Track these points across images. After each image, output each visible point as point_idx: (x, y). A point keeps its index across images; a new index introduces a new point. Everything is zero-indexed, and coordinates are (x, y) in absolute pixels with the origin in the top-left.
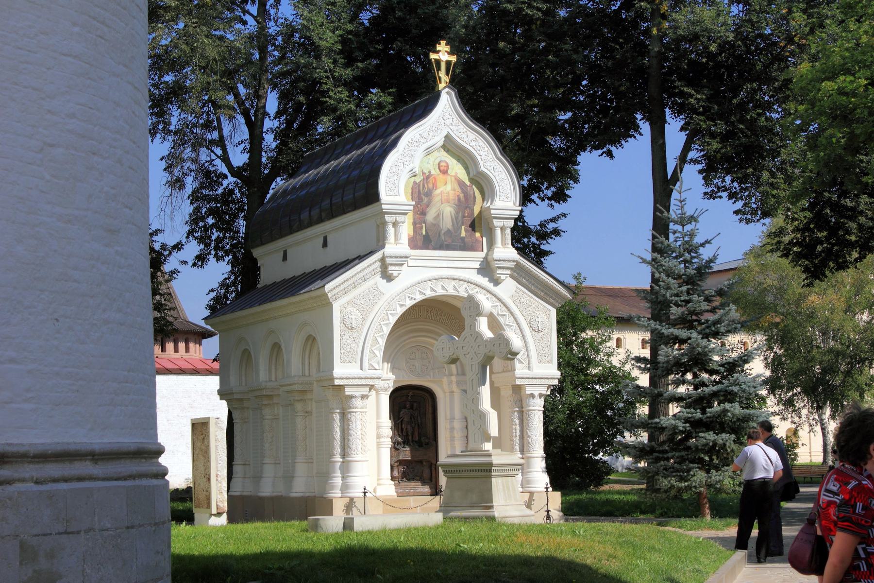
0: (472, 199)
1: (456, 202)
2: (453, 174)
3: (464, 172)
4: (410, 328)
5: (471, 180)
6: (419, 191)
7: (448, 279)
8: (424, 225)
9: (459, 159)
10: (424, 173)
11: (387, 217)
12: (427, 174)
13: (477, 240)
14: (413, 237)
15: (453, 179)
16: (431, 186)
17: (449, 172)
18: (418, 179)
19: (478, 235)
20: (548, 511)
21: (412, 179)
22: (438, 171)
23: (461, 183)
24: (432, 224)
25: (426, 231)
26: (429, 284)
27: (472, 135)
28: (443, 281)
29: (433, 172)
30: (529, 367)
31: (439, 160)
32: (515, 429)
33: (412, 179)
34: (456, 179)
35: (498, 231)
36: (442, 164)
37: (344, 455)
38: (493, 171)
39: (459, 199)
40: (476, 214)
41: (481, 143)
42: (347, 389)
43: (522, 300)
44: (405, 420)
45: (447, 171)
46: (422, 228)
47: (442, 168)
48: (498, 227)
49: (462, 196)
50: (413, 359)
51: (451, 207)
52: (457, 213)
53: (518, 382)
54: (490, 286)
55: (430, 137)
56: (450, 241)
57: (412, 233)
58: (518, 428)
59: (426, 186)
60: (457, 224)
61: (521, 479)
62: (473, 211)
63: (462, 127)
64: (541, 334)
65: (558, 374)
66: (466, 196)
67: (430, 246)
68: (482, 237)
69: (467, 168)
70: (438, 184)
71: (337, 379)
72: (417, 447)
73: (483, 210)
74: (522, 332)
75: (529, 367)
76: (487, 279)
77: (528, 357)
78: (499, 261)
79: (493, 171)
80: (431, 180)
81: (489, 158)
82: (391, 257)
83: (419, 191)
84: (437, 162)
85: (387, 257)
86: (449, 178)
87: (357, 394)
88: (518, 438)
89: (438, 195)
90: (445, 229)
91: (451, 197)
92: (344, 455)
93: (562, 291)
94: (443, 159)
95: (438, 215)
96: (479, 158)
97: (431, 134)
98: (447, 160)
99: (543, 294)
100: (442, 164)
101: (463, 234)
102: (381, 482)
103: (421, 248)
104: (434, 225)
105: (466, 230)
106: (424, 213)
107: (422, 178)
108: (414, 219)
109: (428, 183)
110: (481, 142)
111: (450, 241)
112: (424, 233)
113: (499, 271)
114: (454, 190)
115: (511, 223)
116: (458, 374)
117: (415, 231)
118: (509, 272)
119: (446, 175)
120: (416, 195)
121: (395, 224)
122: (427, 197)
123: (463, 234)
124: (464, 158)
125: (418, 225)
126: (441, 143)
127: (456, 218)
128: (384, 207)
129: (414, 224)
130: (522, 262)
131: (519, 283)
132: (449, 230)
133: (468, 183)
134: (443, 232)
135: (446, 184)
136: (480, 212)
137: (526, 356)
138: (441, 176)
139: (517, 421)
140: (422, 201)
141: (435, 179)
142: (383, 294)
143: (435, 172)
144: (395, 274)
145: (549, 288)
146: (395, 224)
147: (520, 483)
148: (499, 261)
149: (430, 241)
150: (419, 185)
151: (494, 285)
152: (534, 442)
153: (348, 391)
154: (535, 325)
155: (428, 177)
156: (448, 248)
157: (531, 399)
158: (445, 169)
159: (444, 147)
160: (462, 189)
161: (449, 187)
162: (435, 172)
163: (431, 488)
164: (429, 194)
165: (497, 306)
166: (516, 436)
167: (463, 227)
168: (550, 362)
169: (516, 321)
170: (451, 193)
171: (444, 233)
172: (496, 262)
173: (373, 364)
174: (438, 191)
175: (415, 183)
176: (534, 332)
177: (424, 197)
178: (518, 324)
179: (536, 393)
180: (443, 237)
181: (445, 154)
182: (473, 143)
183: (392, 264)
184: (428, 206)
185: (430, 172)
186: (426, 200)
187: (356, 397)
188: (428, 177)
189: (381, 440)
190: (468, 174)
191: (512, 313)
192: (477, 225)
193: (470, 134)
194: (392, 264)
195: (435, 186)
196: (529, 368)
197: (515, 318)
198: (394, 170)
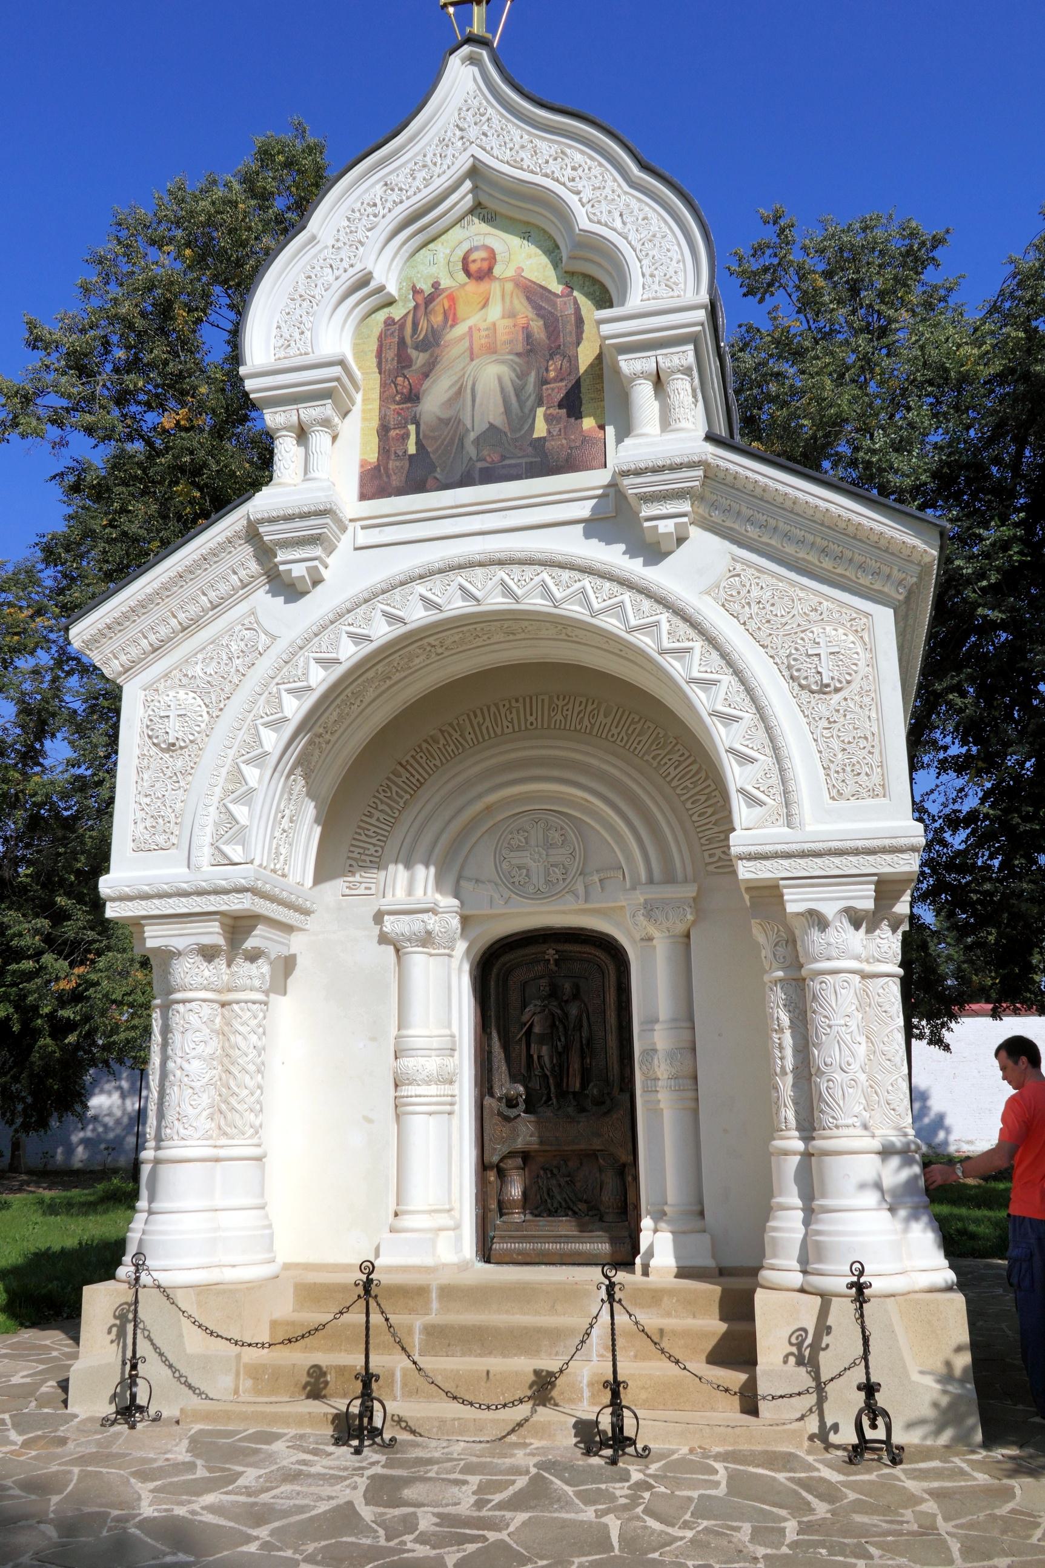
0: (571, 327)
1: (520, 348)
2: (510, 273)
3: (544, 260)
4: (494, 761)
5: (571, 278)
6: (402, 343)
7: (481, 564)
8: (412, 428)
9: (528, 231)
10: (416, 291)
11: (273, 418)
12: (427, 288)
13: (586, 440)
14: (377, 468)
15: (509, 286)
16: (437, 319)
17: (497, 271)
18: (397, 312)
19: (588, 423)
20: (870, 1389)
21: (381, 316)
22: (462, 277)
23: (534, 294)
24: (440, 419)
25: (418, 443)
26: (421, 589)
27: (547, 146)
28: (464, 572)
29: (445, 283)
30: (789, 815)
31: (466, 247)
32: (781, 1047)
33: (381, 316)
34: (517, 285)
35: (644, 392)
36: (473, 256)
37: (808, 1127)
38: (618, 224)
39: (528, 337)
40: (582, 368)
41: (578, 157)
42: (149, 931)
43: (755, 593)
44: (537, 1030)
45: (490, 270)
46: (407, 435)
47: (473, 267)
48: (636, 376)
49: (537, 326)
50: (519, 848)
51: (503, 362)
52: (522, 376)
53: (745, 871)
54: (634, 567)
55: (417, 183)
56: (496, 457)
57: (373, 457)
58: (788, 1039)
59: (423, 324)
60: (521, 403)
61: (799, 1235)
62: (573, 360)
63: (517, 132)
64: (837, 697)
65: (916, 833)
66: (552, 324)
67: (430, 482)
68: (602, 427)
69: (552, 250)
70: (461, 309)
71: (113, 900)
72: (570, 1110)
73: (605, 351)
74: (754, 700)
75: (789, 815)
76: (622, 547)
77: (784, 782)
78: (638, 473)
79: (618, 224)
80: (440, 305)
81: (608, 191)
82: (272, 520)
83: (402, 343)
84: (460, 253)
85: (261, 521)
86: (495, 287)
87: (179, 944)
88: (790, 1079)
89: (461, 338)
90: (480, 427)
91: (502, 335)
92: (808, 1127)
93: (889, 532)
94: (478, 241)
95: (459, 392)
96: (572, 200)
97: (421, 175)
98: (491, 242)
99: (827, 564)
100: (474, 256)
101: (541, 429)
102: (407, 1221)
103: (401, 492)
104: (444, 422)
105: (548, 419)
106: (413, 397)
107: (413, 304)
108: (383, 418)
109: (426, 314)
110: (578, 155)
111: (496, 457)
112: (412, 449)
113: (647, 511)
114: (511, 314)
115: (686, 355)
116: (651, 881)
117: (384, 451)
118: (686, 506)
119: (483, 286)
120: (390, 354)
121: (302, 434)
122: (424, 351)
123: (541, 429)
124: (543, 226)
125: (393, 433)
126: (463, 199)
127: (518, 391)
128: (249, 385)
129: (383, 430)
130: (721, 463)
131: (740, 544)
132: (491, 425)
133: (557, 288)
134: (472, 436)
135: (485, 305)
136: (600, 358)
137: (775, 780)
138: (472, 287)
139: (785, 1019)
140: (410, 366)
141: (452, 299)
142: (274, 638)
143: (452, 280)
144: (298, 571)
145: (876, 546)
146: (302, 434)
147: (795, 1252)
148: (638, 473)
149: (432, 468)
150: (402, 326)
151: (646, 564)
152: (838, 1095)
153: (154, 938)
154: (807, 668)
155: (430, 300)
156: (488, 476)
157: (815, 935)
158: (485, 265)
159: (478, 210)
160: (538, 309)
161: (495, 312)
162: (452, 280)
163: (613, 1241)
164: (431, 342)
165: (657, 624)
166: (784, 1073)
167: (540, 412)
168: (882, 790)
169: (730, 664)
170: (504, 326)
171: (477, 441)
172: (627, 481)
173: (226, 849)
174: (460, 329)
175: (389, 322)
176: (805, 695)
177: (413, 353)
178: (737, 673)
179: (829, 910)
180: (471, 450)
181: (484, 228)
182: (553, 166)
183: (286, 544)
184: (426, 375)
185: (436, 285)
186: (420, 359)
187: (179, 954)
188: (430, 300)
189: (406, 1090)
190: (556, 263)
191: (711, 641)
192: (586, 394)
193: (542, 146)
194: (286, 544)
195: (451, 318)
196: (789, 817)
197: (724, 656)
198: (301, 291)
